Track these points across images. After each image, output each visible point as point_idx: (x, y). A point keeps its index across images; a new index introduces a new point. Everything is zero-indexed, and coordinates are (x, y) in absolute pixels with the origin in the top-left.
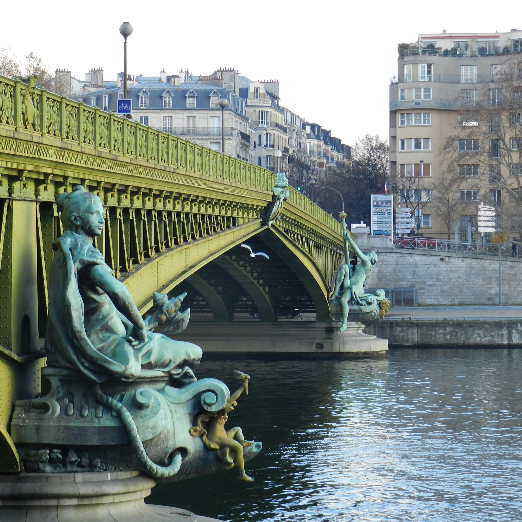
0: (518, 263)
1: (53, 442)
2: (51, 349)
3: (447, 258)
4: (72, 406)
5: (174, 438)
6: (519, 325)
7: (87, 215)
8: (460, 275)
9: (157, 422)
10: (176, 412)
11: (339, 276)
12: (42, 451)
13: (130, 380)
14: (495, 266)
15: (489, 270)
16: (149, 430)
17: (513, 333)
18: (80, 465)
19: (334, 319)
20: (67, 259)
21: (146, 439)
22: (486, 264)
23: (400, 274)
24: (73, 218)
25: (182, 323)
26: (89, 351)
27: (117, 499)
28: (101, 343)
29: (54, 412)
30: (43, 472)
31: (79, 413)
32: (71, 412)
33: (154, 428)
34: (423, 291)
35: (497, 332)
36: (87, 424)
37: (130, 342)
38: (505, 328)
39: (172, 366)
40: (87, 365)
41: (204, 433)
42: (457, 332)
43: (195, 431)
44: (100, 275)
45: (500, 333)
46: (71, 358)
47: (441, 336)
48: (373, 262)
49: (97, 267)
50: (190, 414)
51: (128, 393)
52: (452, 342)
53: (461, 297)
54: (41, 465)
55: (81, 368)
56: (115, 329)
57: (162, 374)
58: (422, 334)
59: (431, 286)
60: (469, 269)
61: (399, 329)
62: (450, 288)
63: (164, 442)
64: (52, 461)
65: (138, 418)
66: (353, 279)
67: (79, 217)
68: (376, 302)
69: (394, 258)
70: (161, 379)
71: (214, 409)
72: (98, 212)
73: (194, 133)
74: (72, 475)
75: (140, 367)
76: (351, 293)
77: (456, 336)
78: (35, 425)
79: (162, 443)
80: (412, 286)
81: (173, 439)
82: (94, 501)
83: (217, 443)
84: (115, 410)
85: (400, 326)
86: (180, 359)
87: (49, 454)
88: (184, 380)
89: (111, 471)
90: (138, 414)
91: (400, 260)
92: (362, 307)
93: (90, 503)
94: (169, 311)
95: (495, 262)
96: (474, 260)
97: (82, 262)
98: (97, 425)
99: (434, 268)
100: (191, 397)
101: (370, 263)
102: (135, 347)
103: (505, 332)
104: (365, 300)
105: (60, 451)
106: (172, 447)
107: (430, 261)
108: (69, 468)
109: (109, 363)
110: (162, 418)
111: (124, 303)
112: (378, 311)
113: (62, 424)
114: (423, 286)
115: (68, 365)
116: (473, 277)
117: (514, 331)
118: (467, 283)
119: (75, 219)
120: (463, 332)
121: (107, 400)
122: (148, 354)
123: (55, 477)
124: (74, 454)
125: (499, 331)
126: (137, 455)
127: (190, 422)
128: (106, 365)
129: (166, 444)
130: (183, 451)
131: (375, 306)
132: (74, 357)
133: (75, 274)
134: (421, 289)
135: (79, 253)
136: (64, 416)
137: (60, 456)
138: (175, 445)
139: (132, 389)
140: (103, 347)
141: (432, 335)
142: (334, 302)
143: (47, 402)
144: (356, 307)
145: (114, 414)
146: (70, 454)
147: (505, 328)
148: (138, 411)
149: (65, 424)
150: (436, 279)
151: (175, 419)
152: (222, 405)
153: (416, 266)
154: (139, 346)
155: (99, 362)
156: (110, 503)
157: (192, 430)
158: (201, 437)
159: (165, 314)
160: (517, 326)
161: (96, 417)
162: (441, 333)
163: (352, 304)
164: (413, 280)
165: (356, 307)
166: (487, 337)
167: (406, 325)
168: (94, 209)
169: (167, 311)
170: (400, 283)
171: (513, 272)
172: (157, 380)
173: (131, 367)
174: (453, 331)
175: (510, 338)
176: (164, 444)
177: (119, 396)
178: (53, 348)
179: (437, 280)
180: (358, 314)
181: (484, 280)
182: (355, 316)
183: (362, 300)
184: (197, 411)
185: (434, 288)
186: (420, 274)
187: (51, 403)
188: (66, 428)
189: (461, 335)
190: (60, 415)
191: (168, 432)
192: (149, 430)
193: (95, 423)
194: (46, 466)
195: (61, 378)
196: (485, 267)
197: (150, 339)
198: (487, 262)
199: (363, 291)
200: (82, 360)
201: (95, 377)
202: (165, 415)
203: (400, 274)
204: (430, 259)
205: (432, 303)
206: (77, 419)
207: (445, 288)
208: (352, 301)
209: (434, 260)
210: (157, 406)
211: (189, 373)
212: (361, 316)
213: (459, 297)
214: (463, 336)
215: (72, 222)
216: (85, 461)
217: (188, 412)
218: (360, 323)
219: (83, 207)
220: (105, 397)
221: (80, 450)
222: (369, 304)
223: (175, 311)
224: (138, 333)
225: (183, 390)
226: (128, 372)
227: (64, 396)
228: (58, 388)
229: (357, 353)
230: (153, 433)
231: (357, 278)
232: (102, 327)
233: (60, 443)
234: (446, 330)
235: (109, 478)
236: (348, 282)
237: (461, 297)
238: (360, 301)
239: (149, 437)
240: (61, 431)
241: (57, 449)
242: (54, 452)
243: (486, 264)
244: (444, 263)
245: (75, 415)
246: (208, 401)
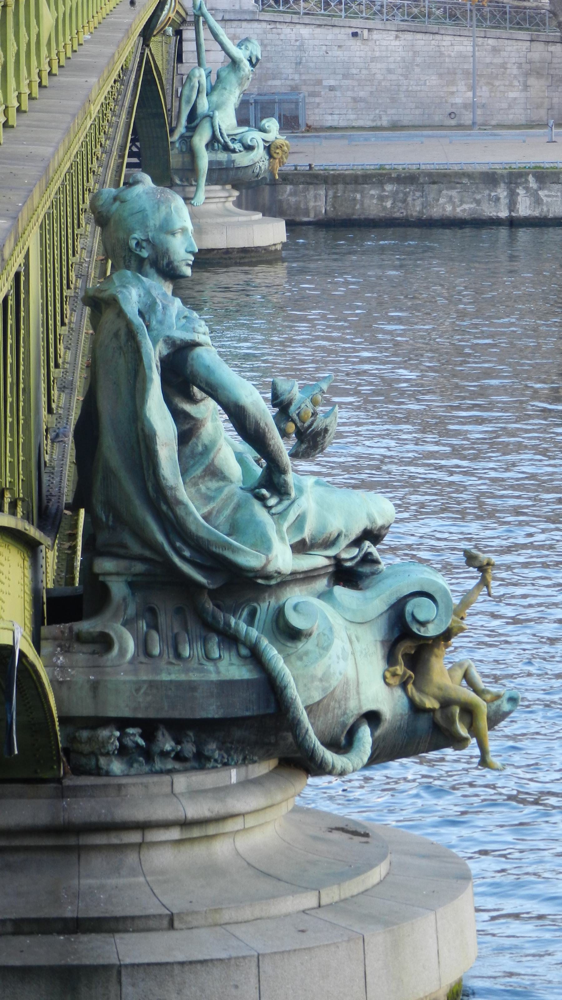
0: (510, 42)
1: (127, 713)
2: (107, 517)
3: (366, 32)
4: (155, 636)
5: (358, 693)
6: (531, 178)
7: (162, 236)
8: (392, 66)
9: (329, 666)
10: (358, 641)
11: (186, 92)
12: (104, 733)
13: (273, 582)
14: (462, 48)
15: (450, 56)
16: (317, 683)
17: (518, 194)
18: (179, 757)
19: (178, 182)
20: (140, 338)
21: (310, 702)
22: (444, 43)
23: (269, 65)
24: (133, 243)
25: (324, 437)
26: (193, 527)
27: (250, 821)
28: (206, 505)
29: (123, 651)
30: (108, 774)
31: (171, 651)
32: (156, 651)
33: (325, 678)
34: (317, 100)
35: (487, 192)
36: (194, 677)
37: (262, 499)
38: (502, 185)
39: (344, 542)
40: (187, 553)
41: (410, 677)
42: (406, 194)
43: (394, 675)
44: (208, 368)
45: (493, 194)
46: (156, 541)
47: (375, 201)
48: (254, 61)
49: (198, 350)
50: (383, 642)
51: (264, 605)
52: (397, 215)
53: (393, 111)
54: (103, 761)
55: (177, 560)
56: (227, 473)
57: (326, 562)
58: (335, 197)
59: (332, 89)
60: (411, 54)
61: (289, 188)
62: (371, 92)
63: (339, 702)
65: (293, 658)
66: (215, 97)
67: (147, 240)
68: (261, 144)
69: (258, 31)
70: (322, 572)
71: (431, 631)
72: (184, 230)
74: (166, 778)
75: (289, 550)
76: (213, 127)
77: (404, 201)
78: (89, 681)
79: (337, 706)
80: (295, 89)
81: (356, 697)
82: (211, 830)
83: (436, 698)
84: (244, 644)
85: (291, 183)
86: (356, 531)
87: (119, 739)
88: (360, 569)
89: (236, 765)
90: (291, 651)
91: (269, 36)
92: (234, 156)
93: (203, 834)
94: (302, 414)
95: (461, 39)
96: (419, 36)
97: (170, 341)
98: (214, 677)
99: (339, 53)
100: (386, 608)
101: (248, 63)
102: (273, 511)
103: (502, 192)
104: (240, 141)
105: (140, 731)
106: (356, 712)
107: (329, 37)
108: (158, 765)
109: (235, 550)
110: (338, 657)
111: (257, 424)
112: (266, 163)
113: (145, 678)
114: (317, 89)
115: (147, 553)
116: (417, 70)
117: (521, 191)
118: (405, 82)
119: (138, 244)
120: (418, 194)
121: (227, 624)
122: (300, 521)
123: (134, 785)
124: (167, 734)
125: (491, 191)
126: (296, 737)
127: (384, 657)
128: (228, 554)
129: (343, 707)
131: (259, 153)
132: (160, 538)
133: (157, 366)
134: (313, 94)
135: (161, 323)
136: (142, 659)
137: (141, 742)
138: (361, 708)
139: (270, 596)
140: (210, 513)
141: (355, 199)
142: (177, 145)
143: (107, 631)
144: (222, 156)
145: (244, 651)
146: (159, 735)
147: (502, 185)
148: (289, 644)
149: (151, 677)
150: (343, 75)
151: (358, 654)
152: (447, 623)
153: (301, 48)
154: (280, 508)
155: (214, 549)
156: (238, 831)
157: (388, 675)
158: (404, 685)
159: (293, 421)
160: (527, 181)
161: (208, 658)
162: (373, 196)
163: (213, 149)
164: (297, 77)
165: (222, 156)
166: (467, 203)
167: (302, 179)
168: (178, 225)
169: (298, 415)
170: (270, 83)
171: (498, 60)
172: (316, 574)
173: (277, 556)
174: (397, 193)
175: (512, 205)
176: (340, 707)
177: (245, 613)
178: (111, 518)
179: (346, 76)
180: (227, 169)
181: (440, 75)
183: (233, 140)
184: (396, 635)
185: (338, 94)
186: (311, 65)
187: (116, 633)
188: (152, 684)
189: (414, 200)
190: (134, 657)
191: (347, 683)
192: (317, 683)
193: (209, 672)
194: (111, 761)
195: (129, 580)
196: (443, 49)
197: (300, 491)
198: (447, 40)
199: (234, 121)
200: (178, 544)
201: (205, 577)
202: (343, 649)
203: (269, 65)
204: (330, 34)
205: (335, 124)
206: (171, 663)
207: (362, 94)
209: (339, 37)
210: (326, 632)
211: (370, 554)
212: (231, 173)
213: (389, 111)
214: (418, 202)
215: (130, 250)
216: (189, 748)
217: (379, 638)
218: (228, 187)
219: (154, 221)
220: (221, 615)
222: (249, 148)
223: (313, 414)
224: (276, 480)
225: (368, 593)
226: (271, 568)
227: (138, 616)
228: (124, 599)
229: (228, 251)
230: (324, 690)
231: (222, 95)
232: (205, 471)
233: (140, 715)
234: (384, 190)
235: (234, 780)
236: (204, 106)
237: (393, 111)
238: (230, 143)
239: (316, 696)
240: (142, 691)
241: (133, 726)
242: (129, 735)
243: (444, 43)
244: (359, 43)
245: (165, 656)
246: (421, 617)
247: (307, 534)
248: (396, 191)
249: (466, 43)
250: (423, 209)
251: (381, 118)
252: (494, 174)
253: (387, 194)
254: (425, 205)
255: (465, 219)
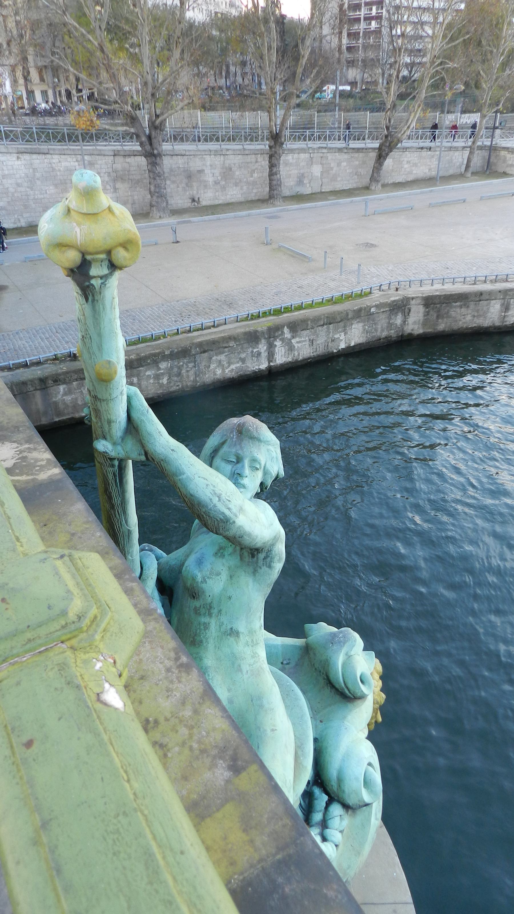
0: (99, 157)
6: (286, 330)
8: (19, 181)
14: (67, 164)
15: (60, 171)
17: (276, 346)
35: (250, 349)
38: (263, 341)
42: (180, 368)
45: (255, 350)
47: (152, 381)
52: (174, 388)
53: (28, 215)
60: (31, 170)
62: (8, 202)
77: (179, 374)
85: (64, 383)
95: (66, 156)
96: (35, 156)
116: (38, 183)
117: (278, 343)
120: (191, 365)
125: (254, 348)
147: (263, 341)
160: (283, 333)
166: (232, 363)
167: (76, 376)
174: (172, 368)
175: (271, 356)
181: (56, 186)
189: (188, 371)
196: (54, 165)
198: (56, 158)
213: (25, 215)
214: (192, 373)
234: (159, 369)
237: (28, 215)
243: (54, 161)
248: (171, 367)
249: (69, 159)
250: (196, 377)
251: (19, 221)
252: (256, 332)
253: (162, 371)
254: (198, 373)
255: (233, 378)
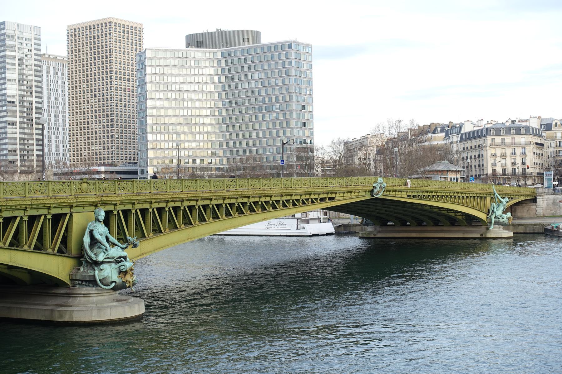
33: (104, 275)
64: (79, 284)
73: (515, 144)
130: (115, 282)
131: (505, 219)
144: (497, 220)
165: (497, 220)
182: (497, 223)
208: (495, 217)
216: (87, 284)
221: (86, 281)
222: (503, 218)
236: (495, 210)
247: (109, 256)
